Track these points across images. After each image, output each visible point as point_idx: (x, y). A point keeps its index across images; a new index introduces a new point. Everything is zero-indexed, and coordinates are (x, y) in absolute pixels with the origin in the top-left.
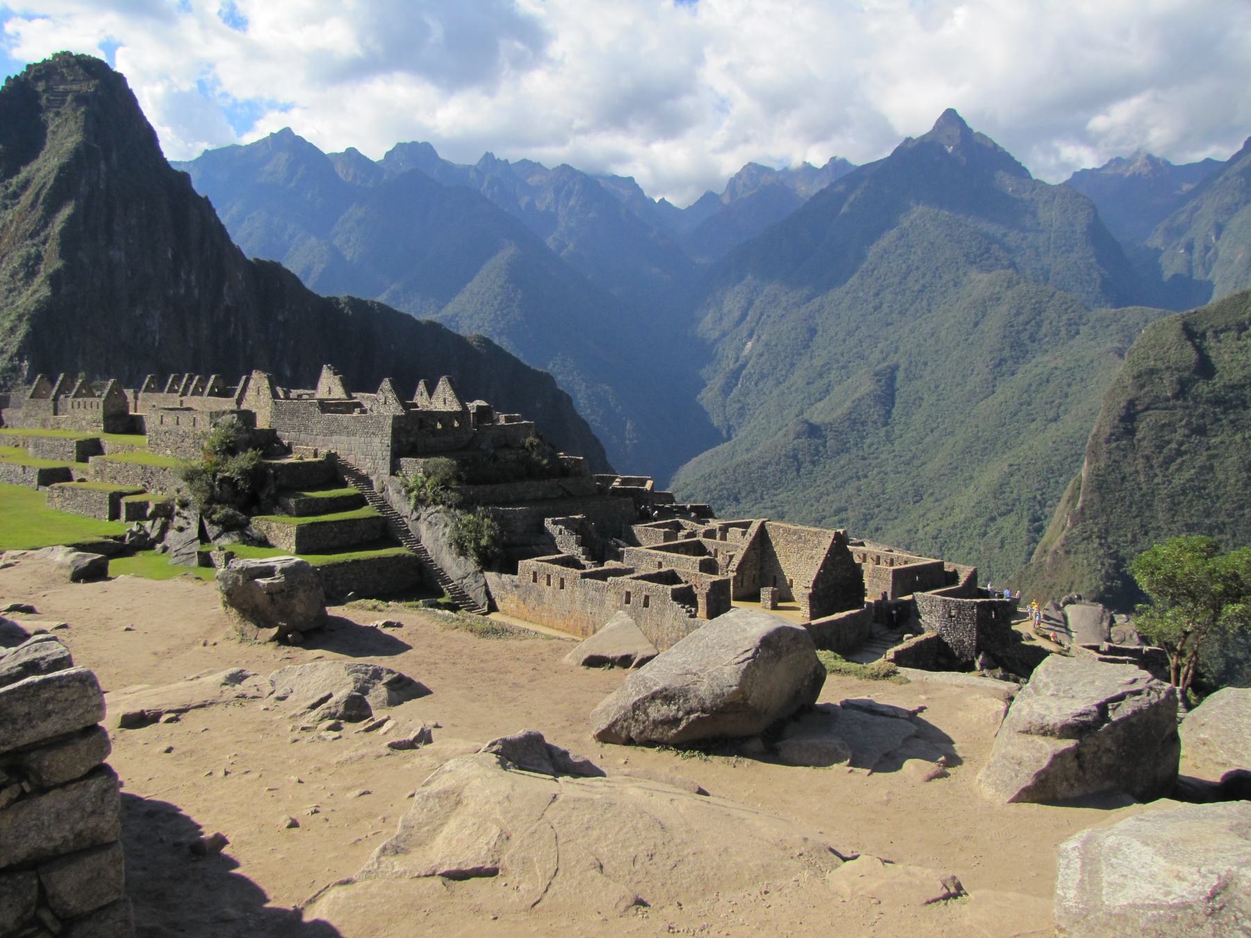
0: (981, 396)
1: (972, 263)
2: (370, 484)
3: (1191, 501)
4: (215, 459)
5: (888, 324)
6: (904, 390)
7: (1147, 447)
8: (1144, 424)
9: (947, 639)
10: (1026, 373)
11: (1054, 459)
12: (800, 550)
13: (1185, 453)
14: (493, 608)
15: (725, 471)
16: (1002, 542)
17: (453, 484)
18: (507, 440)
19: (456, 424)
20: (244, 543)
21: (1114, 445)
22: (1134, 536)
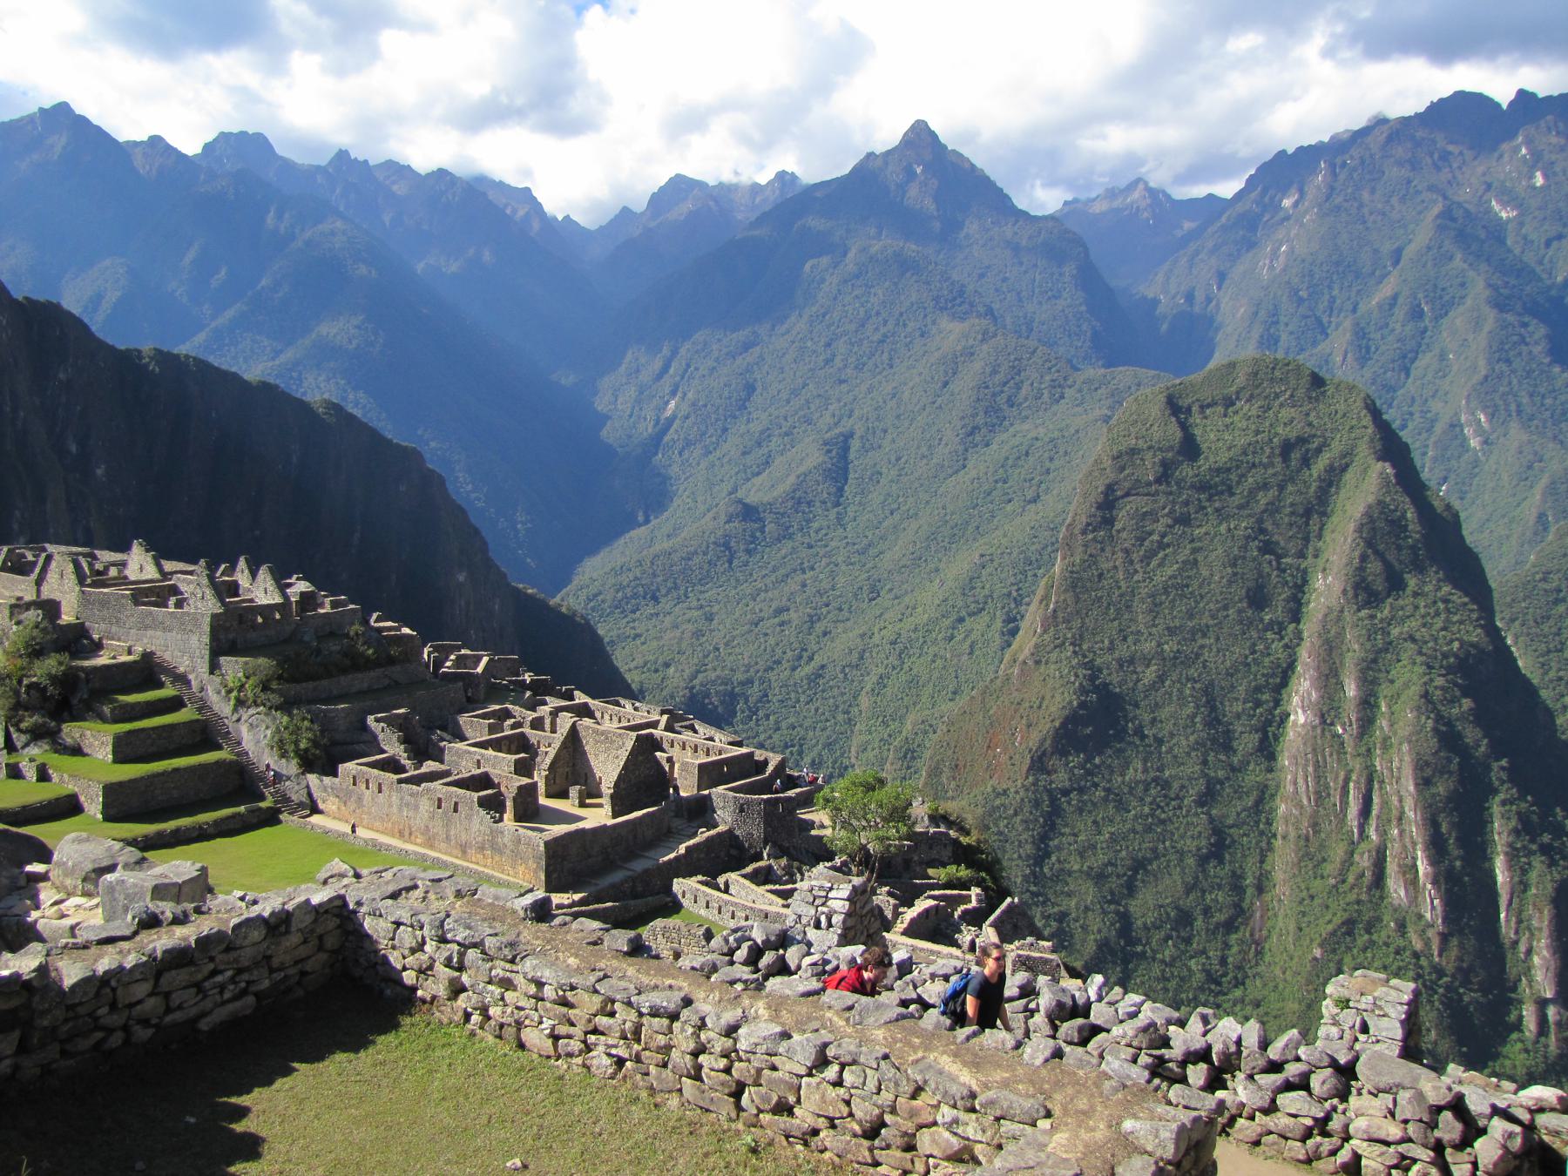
0: (950, 471)
1: (941, 309)
2: (188, 683)
3: (1174, 601)
4: (19, 662)
5: (841, 382)
6: (859, 462)
7: (1127, 539)
8: (1123, 513)
9: (738, 832)
10: (1004, 443)
11: (1033, 548)
12: (607, 749)
13: (1168, 545)
14: (315, 810)
15: (640, 563)
16: (972, 646)
17: (274, 686)
18: (331, 629)
19: (278, 616)
20: (56, 751)
21: (1090, 537)
22: (1111, 642)
